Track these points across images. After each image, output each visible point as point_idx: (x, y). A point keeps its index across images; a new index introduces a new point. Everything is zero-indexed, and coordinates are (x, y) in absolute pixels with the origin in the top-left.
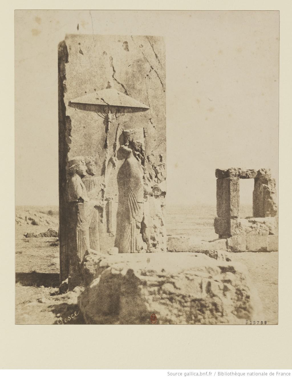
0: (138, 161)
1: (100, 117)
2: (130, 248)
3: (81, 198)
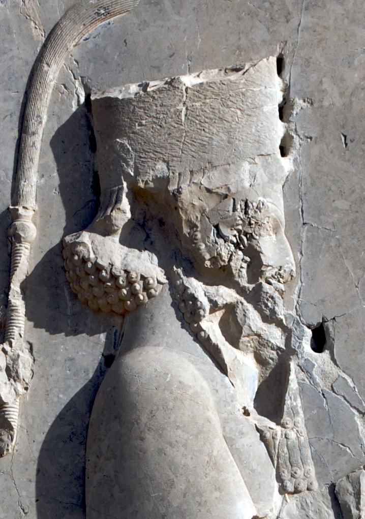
0: (222, 367)
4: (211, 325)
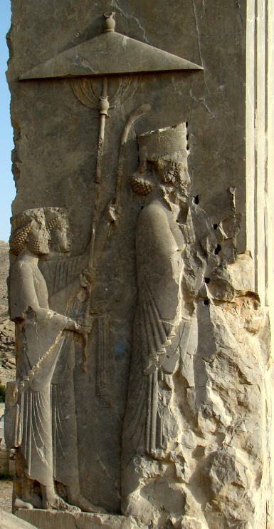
1: (82, 106)
2: (142, 439)
3: (30, 308)
4: (166, 197)
